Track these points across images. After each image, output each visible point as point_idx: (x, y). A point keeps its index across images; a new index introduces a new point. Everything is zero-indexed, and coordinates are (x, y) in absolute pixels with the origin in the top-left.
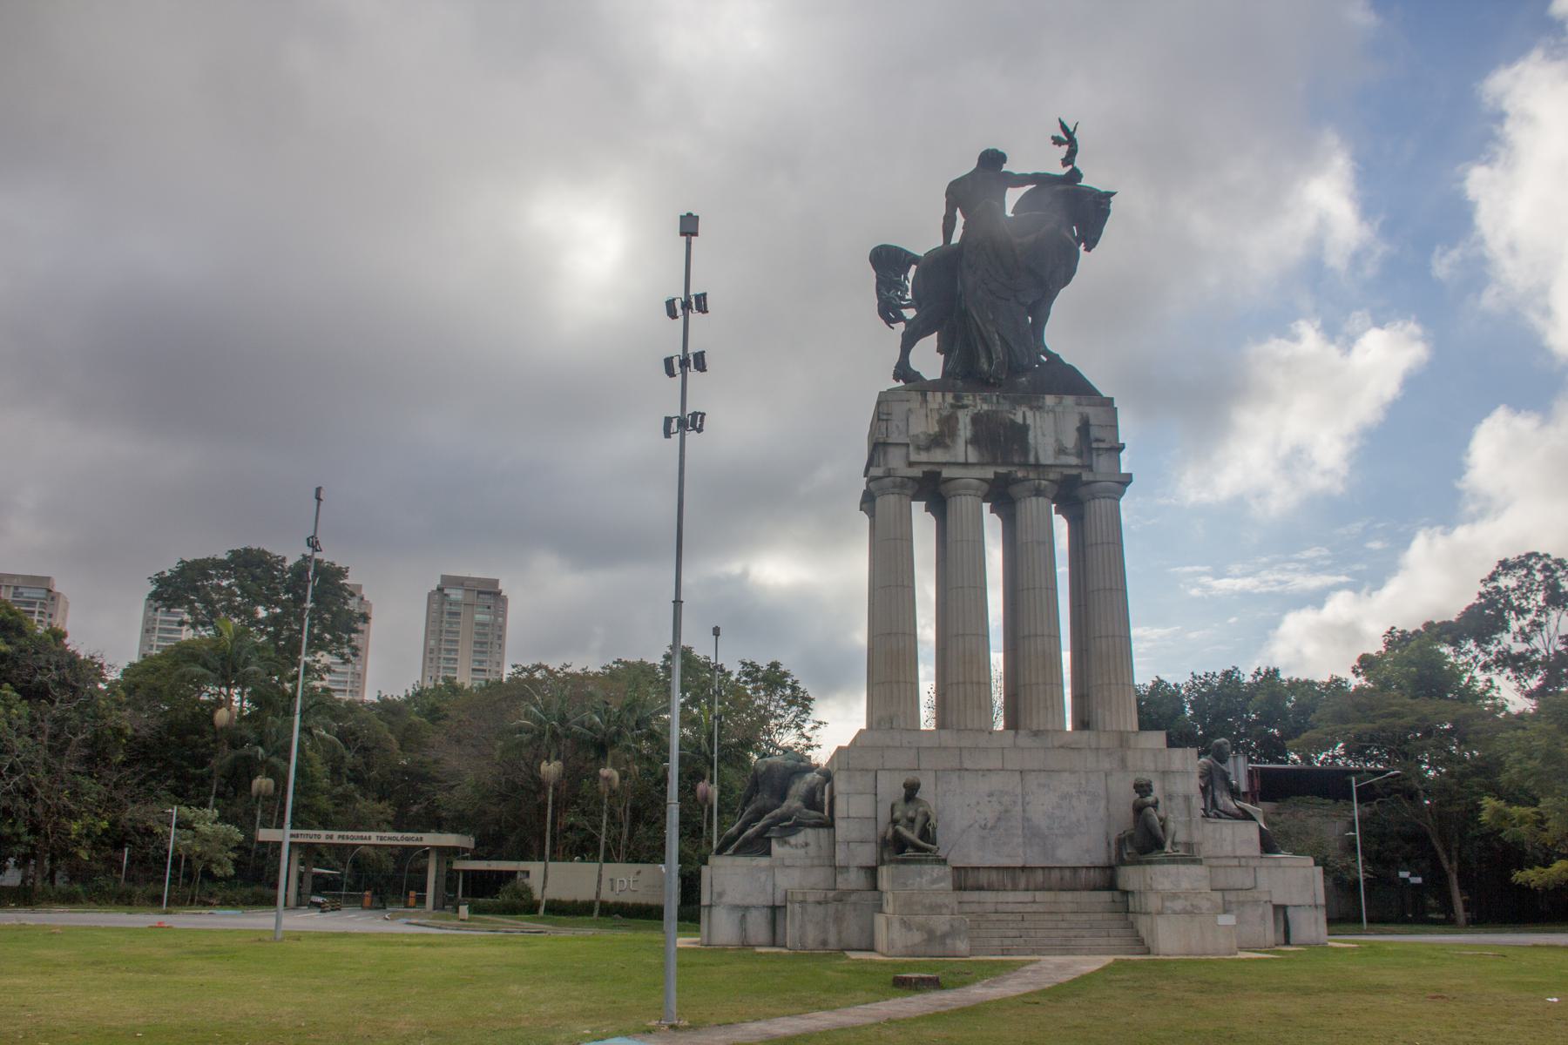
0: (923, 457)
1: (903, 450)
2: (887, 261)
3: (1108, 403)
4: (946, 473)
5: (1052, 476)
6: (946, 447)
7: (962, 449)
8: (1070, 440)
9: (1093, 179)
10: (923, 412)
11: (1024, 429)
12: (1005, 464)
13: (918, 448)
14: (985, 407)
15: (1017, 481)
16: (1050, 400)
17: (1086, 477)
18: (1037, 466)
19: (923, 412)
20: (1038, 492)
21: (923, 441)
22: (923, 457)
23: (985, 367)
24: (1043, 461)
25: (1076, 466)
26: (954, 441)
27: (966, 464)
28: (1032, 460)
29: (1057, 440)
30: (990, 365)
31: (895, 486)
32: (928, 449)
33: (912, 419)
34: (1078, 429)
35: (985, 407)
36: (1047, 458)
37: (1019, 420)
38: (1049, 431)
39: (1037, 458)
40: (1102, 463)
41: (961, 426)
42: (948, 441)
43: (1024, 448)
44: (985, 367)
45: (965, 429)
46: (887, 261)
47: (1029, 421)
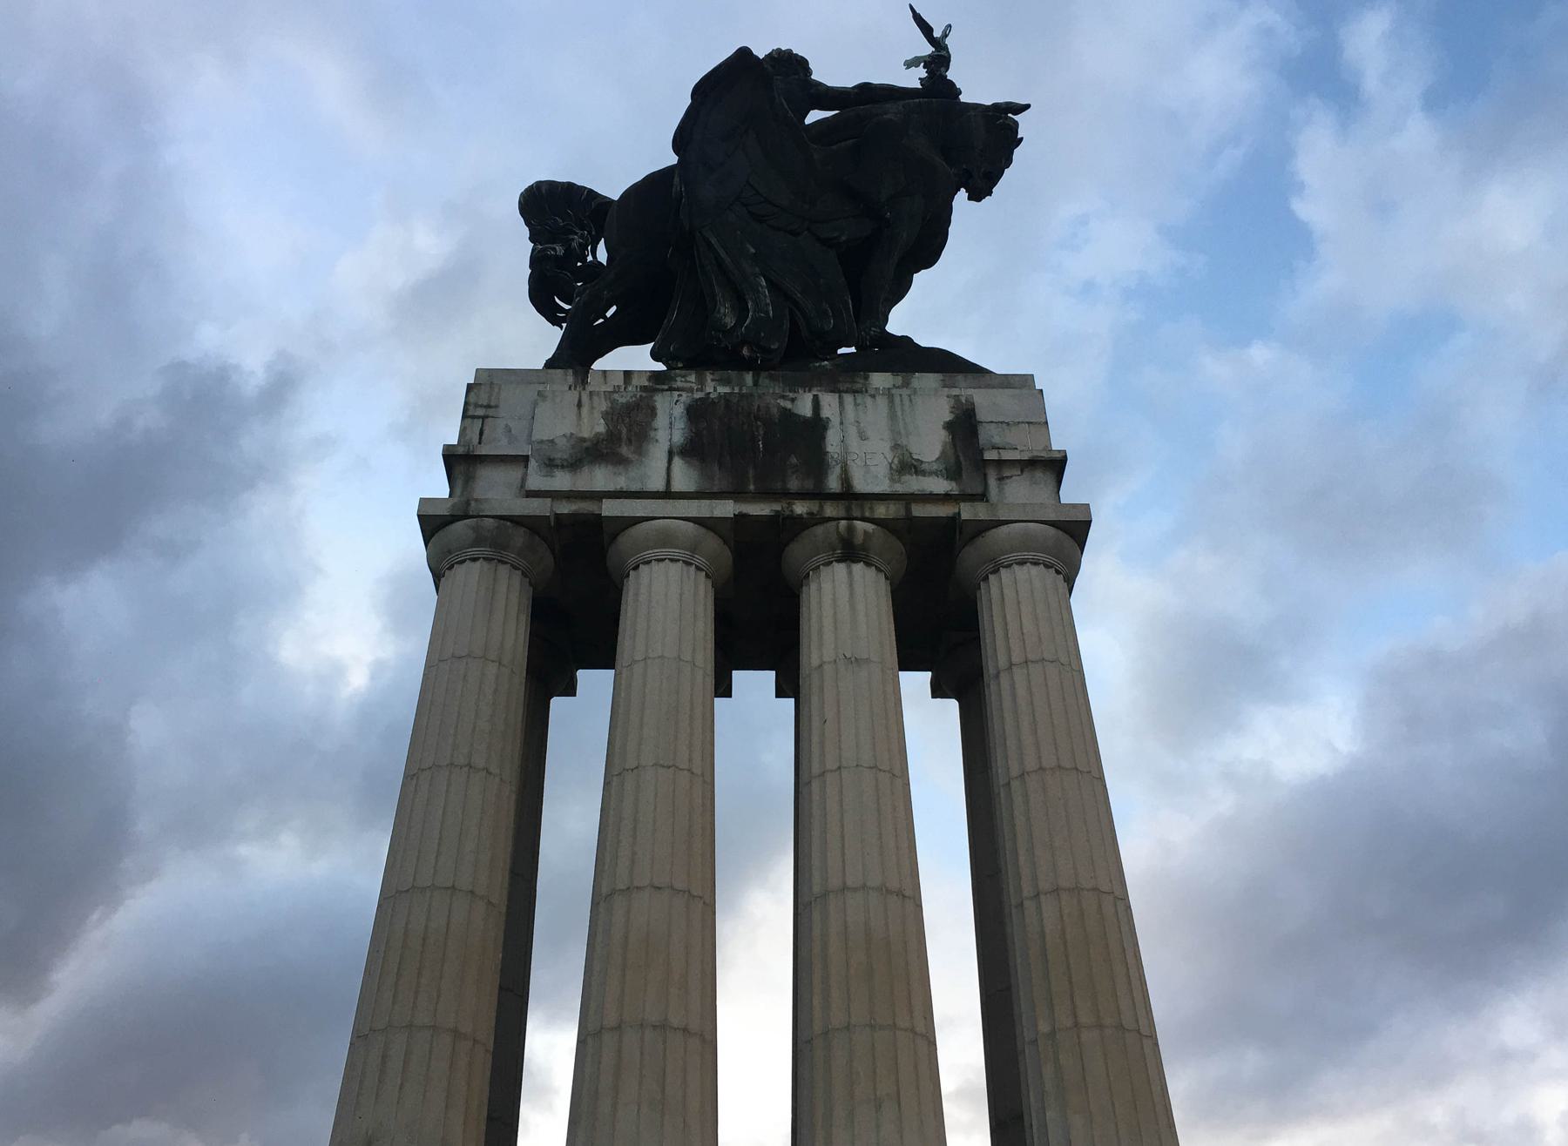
0: (562, 481)
1: (512, 474)
2: (553, 210)
3: (1026, 381)
4: (610, 508)
5: (881, 511)
6: (620, 461)
7: (656, 466)
8: (930, 443)
9: (976, 84)
10: (573, 396)
11: (817, 426)
12: (764, 495)
13: (550, 465)
14: (723, 390)
15: (800, 525)
16: (880, 380)
17: (967, 512)
18: (848, 495)
19: (573, 396)
20: (850, 552)
21: (563, 451)
22: (562, 481)
23: (730, 321)
24: (861, 485)
25: (946, 498)
26: (640, 451)
27: (667, 494)
28: (833, 484)
29: (896, 447)
30: (740, 320)
31: (478, 542)
32: (574, 465)
33: (544, 410)
34: (949, 426)
35: (723, 390)
36: (872, 475)
37: (804, 407)
38: (873, 440)
39: (846, 479)
40: (1017, 495)
41: (661, 421)
42: (625, 450)
43: (817, 461)
44: (730, 321)
45: (670, 421)
46: (553, 210)
47: (826, 413)
